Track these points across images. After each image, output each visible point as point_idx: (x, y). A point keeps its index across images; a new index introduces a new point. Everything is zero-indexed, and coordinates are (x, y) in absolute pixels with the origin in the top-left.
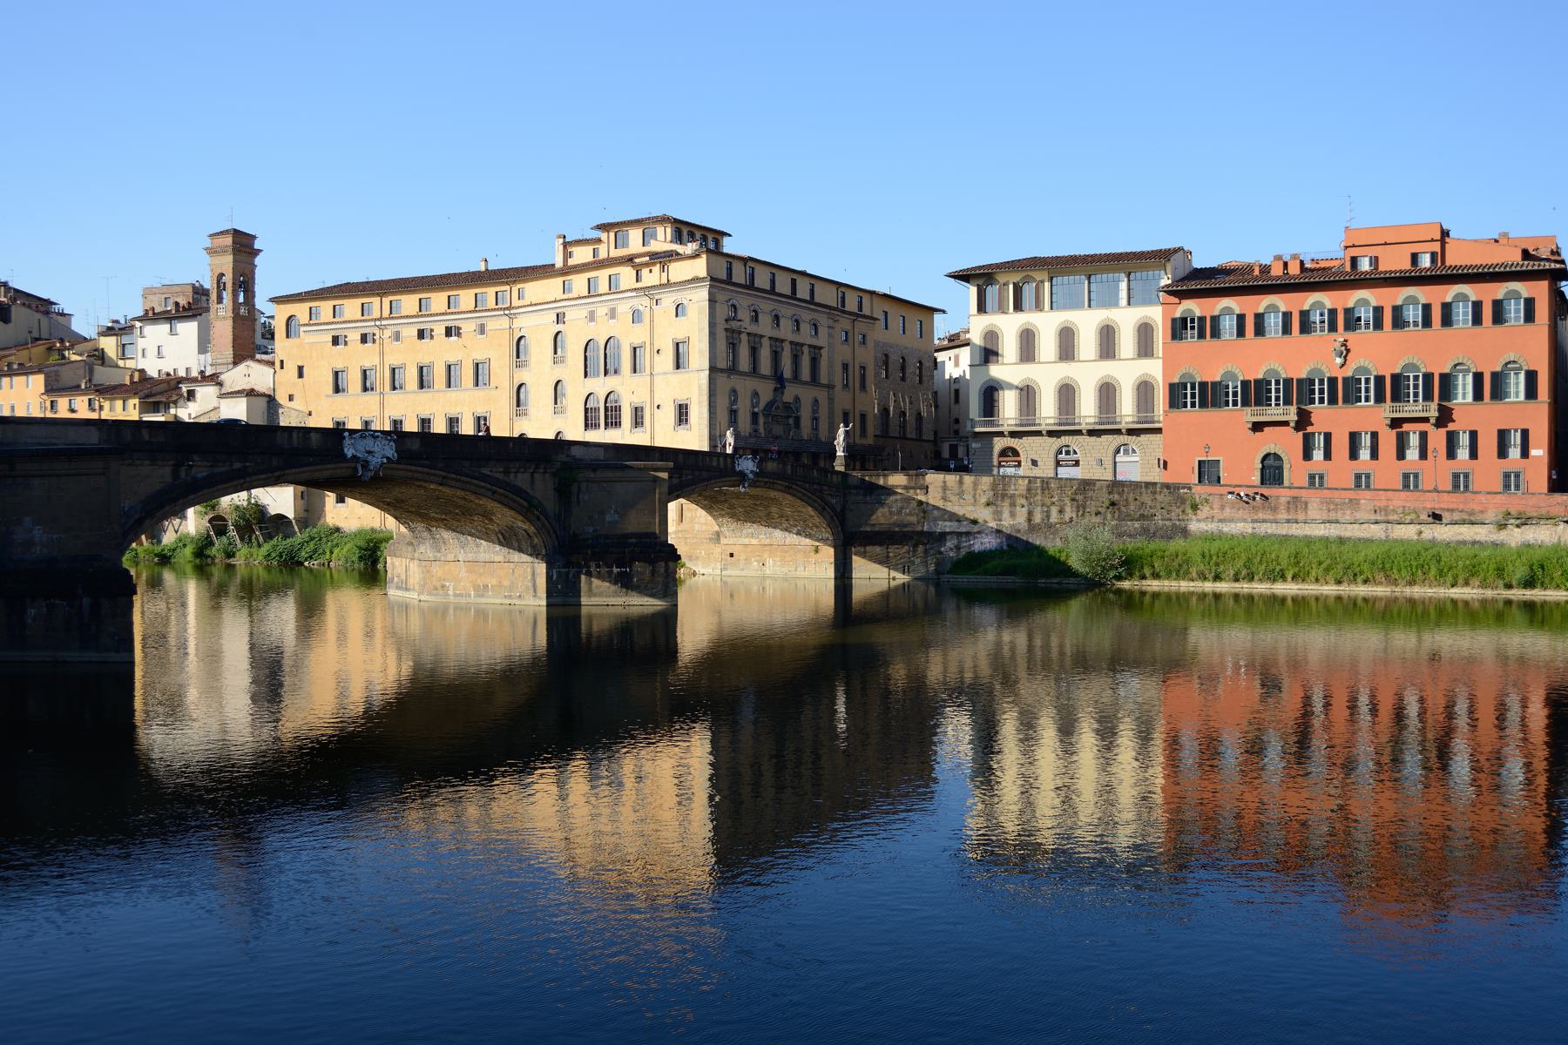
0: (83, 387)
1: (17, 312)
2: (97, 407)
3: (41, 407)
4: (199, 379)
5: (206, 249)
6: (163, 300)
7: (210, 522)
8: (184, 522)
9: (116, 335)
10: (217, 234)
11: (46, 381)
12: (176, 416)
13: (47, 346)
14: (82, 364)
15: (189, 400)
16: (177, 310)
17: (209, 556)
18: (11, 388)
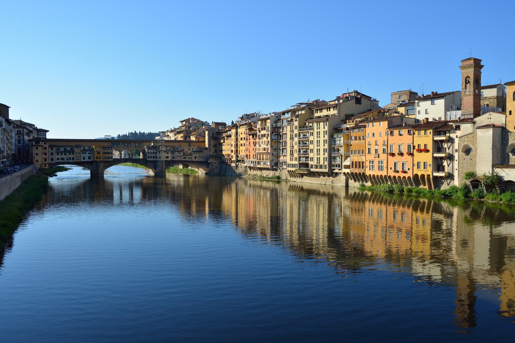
0: (404, 125)
1: (363, 100)
2: (412, 133)
3: (386, 134)
4: (458, 121)
5: (460, 67)
6: (398, 96)
7: (471, 182)
8: (452, 181)
9: (405, 106)
10: (466, 60)
11: (388, 123)
12: (449, 136)
13: (378, 111)
14: (399, 117)
15: (456, 130)
16: (433, 95)
17: (470, 197)
18: (373, 126)
